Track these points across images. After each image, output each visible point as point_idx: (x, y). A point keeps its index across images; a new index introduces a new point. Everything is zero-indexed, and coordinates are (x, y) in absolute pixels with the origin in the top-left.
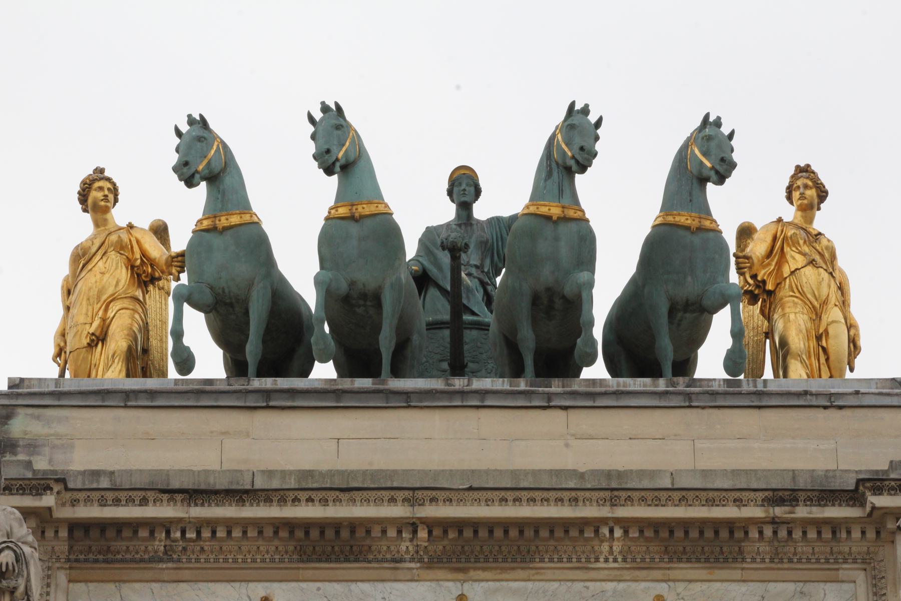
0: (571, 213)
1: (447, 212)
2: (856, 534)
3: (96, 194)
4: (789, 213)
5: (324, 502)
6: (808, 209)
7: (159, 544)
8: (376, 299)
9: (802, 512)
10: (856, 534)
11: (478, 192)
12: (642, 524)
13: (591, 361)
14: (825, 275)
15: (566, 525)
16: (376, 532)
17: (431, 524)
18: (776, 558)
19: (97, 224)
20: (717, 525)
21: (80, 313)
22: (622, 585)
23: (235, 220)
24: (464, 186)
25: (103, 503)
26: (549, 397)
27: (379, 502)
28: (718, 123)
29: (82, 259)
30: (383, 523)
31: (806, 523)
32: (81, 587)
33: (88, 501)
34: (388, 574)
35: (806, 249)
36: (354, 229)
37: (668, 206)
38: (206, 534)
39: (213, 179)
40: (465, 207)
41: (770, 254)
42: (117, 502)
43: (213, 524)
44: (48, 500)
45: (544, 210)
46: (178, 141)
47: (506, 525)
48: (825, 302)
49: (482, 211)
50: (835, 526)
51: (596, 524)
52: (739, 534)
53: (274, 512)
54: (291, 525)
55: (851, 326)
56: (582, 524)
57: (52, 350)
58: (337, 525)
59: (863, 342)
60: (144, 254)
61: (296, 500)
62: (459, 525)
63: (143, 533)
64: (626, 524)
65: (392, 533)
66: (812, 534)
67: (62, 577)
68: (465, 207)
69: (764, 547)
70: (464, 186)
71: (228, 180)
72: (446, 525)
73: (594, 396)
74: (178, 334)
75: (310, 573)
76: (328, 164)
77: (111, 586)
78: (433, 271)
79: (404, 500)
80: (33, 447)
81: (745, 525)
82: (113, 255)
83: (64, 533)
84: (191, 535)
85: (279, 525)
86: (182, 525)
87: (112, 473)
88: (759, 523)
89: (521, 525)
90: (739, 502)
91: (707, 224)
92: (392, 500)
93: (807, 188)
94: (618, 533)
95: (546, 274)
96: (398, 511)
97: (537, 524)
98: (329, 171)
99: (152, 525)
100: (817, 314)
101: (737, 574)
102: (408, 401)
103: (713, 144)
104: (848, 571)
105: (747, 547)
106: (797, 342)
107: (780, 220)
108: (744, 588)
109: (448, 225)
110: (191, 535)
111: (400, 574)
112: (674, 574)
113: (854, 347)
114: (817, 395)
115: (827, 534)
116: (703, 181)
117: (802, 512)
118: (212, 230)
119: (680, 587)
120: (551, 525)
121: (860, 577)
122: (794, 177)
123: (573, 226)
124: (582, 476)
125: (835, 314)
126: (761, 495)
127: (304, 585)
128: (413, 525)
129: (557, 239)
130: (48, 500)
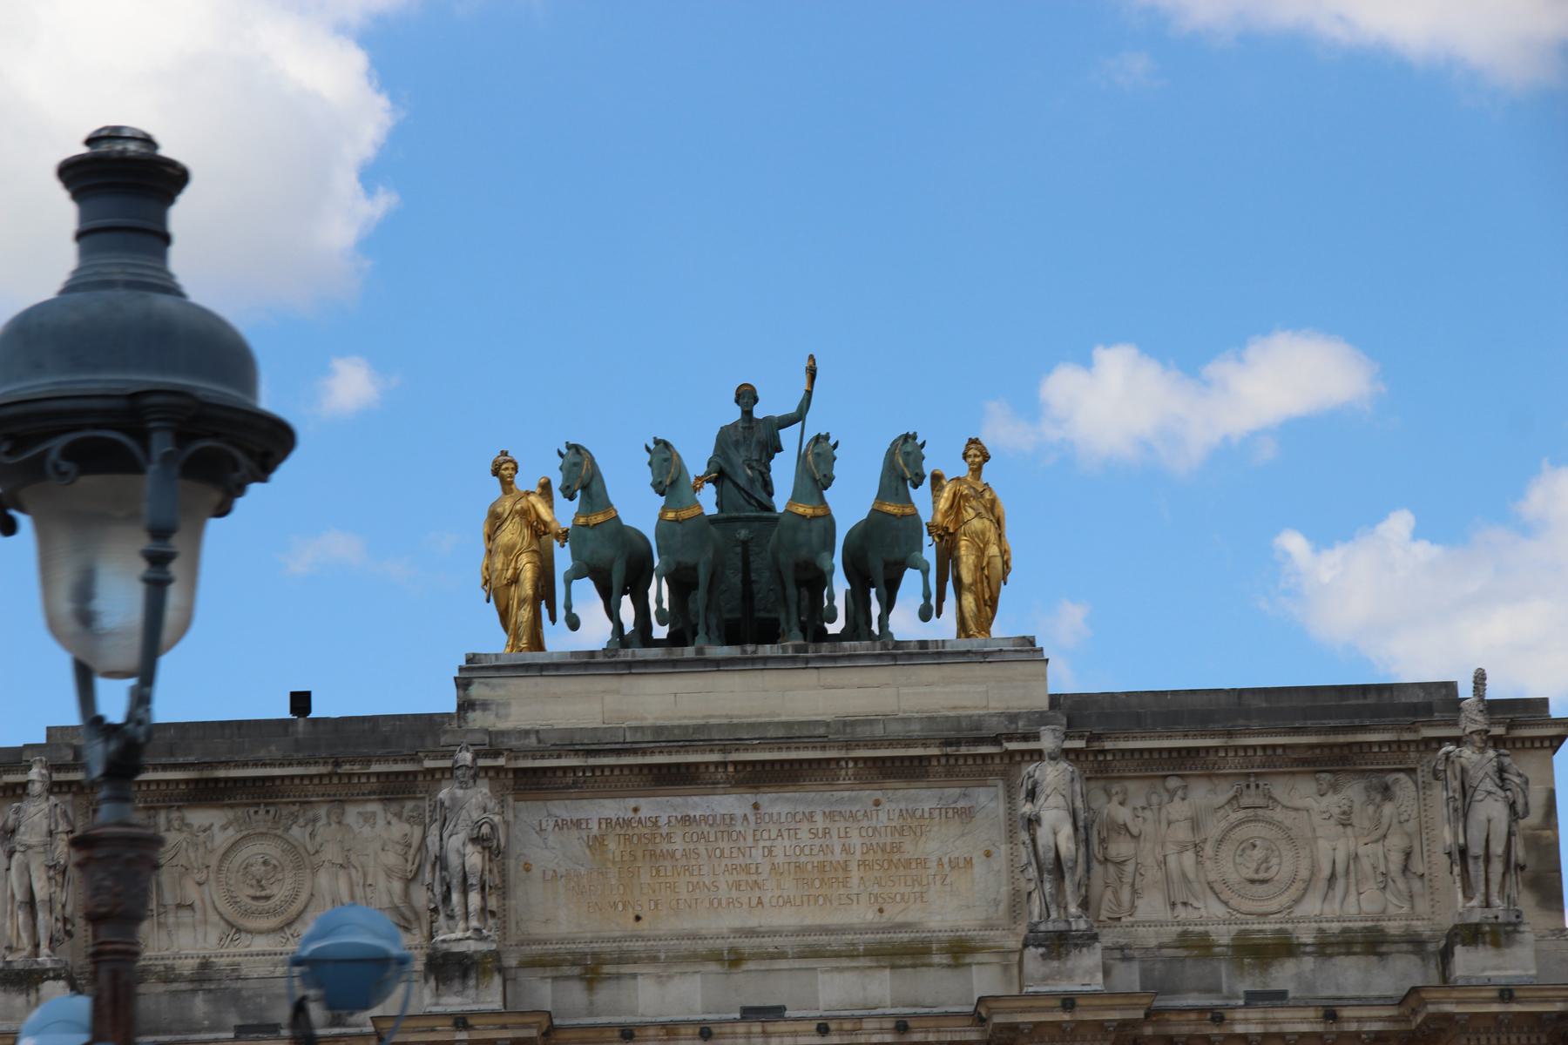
0: (819, 512)
1: (734, 414)
2: (997, 760)
3: (504, 470)
4: (963, 470)
5: (670, 753)
6: (977, 471)
7: (569, 779)
8: (695, 568)
9: (964, 750)
10: (997, 760)
11: (756, 400)
12: (865, 760)
13: (832, 620)
14: (987, 523)
15: (819, 761)
16: (702, 769)
17: (735, 763)
19: (505, 492)
20: (911, 758)
21: (499, 562)
23: (600, 518)
24: (746, 396)
25: (534, 758)
26: (807, 660)
27: (703, 752)
28: (914, 437)
29: (496, 521)
30: (707, 764)
31: (966, 756)
32: (521, 804)
33: (525, 757)
35: (974, 503)
36: (678, 528)
37: (881, 497)
39: (585, 488)
40: (747, 413)
41: (951, 506)
42: (543, 757)
43: (602, 768)
44: (501, 761)
45: (801, 510)
46: (560, 461)
48: (986, 543)
49: (759, 412)
50: (984, 756)
53: (640, 760)
54: (650, 767)
55: (1004, 552)
56: (828, 760)
57: (480, 581)
58: (678, 765)
59: (1012, 564)
60: (538, 516)
61: (652, 753)
62: (753, 763)
63: (560, 774)
64: (856, 760)
65: (712, 769)
66: (970, 761)
67: (510, 799)
68: (747, 413)
70: (746, 396)
71: (595, 487)
72: (745, 763)
74: (568, 607)
76: (660, 488)
77: (540, 803)
78: (728, 469)
80: (485, 705)
81: (929, 758)
82: (517, 519)
83: (511, 775)
85: (641, 767)
86: (584, 769)
87: (537, 732)
88: (938, 757)
90: (925, 745)
91: (908, 511)
92: (712, 751)
93: (977, 454)
95: (804, 554)
96: (715, 757)
97: (801, 762)
98: (662, 494)
99: (565, 769)
100: (981, 552)
101: (924, 784)
102: (718, 664)
103: (911, 458)
104: (991, 780)
106: (967, 578)
107: (958, 479)
108: (929, 792)
109: (735, 425)
112: (887, 785)
113: (1006, 564)
114: (976, 653)
115: (979, 761)
116: (904, 480)
117: (964, 750)
118: (586, 525)
119: (890, 793)
120: (810, 761)
121: (1000, 784)
122: (968, 448)
123: (821, 521)
124: (827, 724)
125: (993, 550)
128: (725, 764)
129: (810, 531)
130: (501, 761)
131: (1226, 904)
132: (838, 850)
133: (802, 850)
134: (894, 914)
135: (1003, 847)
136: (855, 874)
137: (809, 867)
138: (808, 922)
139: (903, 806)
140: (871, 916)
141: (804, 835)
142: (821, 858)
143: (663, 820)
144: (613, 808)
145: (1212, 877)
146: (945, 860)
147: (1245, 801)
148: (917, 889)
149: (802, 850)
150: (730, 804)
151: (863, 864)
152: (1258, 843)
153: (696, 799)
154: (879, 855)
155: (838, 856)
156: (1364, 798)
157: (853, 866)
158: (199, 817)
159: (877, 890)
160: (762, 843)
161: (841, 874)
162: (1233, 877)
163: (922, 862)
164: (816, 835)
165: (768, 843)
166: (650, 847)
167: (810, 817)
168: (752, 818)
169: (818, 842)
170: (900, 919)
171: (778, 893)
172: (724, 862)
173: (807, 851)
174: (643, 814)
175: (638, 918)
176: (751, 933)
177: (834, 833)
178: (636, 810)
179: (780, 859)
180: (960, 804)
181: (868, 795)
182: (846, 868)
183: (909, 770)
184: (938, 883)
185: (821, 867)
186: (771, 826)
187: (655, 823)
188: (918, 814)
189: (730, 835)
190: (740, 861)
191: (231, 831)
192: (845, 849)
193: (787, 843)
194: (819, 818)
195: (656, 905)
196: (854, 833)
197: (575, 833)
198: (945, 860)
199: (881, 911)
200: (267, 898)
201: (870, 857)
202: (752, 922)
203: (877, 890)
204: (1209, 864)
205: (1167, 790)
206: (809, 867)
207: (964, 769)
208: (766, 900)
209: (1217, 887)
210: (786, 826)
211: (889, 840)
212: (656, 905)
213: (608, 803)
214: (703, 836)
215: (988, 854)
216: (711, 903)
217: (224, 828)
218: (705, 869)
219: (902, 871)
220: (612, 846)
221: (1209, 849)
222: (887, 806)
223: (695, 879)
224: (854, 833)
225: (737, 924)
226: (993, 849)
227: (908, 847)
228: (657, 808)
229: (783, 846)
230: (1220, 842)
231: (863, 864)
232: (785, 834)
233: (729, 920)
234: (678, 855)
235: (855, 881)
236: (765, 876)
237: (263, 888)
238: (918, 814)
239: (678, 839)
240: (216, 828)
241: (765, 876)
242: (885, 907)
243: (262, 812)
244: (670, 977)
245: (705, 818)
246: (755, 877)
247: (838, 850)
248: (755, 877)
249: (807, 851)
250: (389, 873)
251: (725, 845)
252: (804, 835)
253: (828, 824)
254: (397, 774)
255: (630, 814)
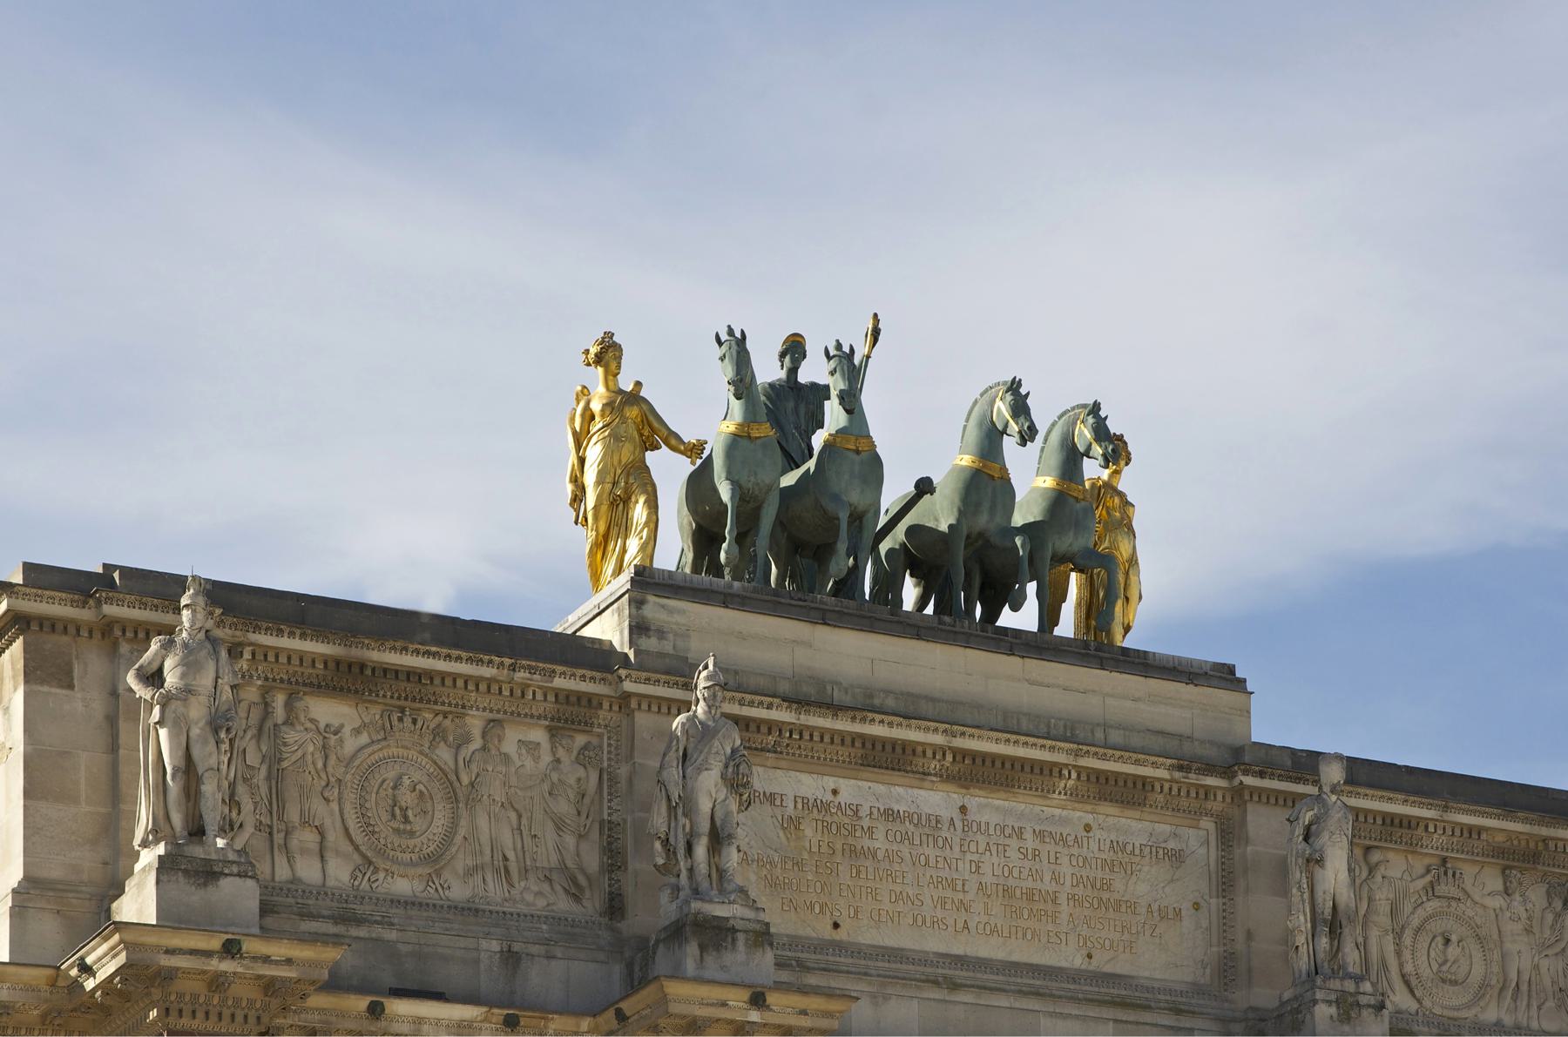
10: (1220, 798)
18: (1165, 807)
22: (1065, 813)
34: (917, 783)
38: (807, 737)
47: (1004, 759)
50: (1208, 792)
51: (1060, 767)
52: (1148, 788)
53: (858, 728)
54: (863, 738)
58: (894, 743)
62: (974, 756)
69: (1161, 798)
73: (1015, 642)
75: (865, 775)
79: (945, 731)
84: (796, 736)
85: (855, 737)
89: (1014, 760)
94: (1074, 775)
96: (939, 739)
101: (1137, 814)
105: (1152, 797)
110: (796, 736)
111: (926, 784)
126: (1169, 761)
127: (860, 783)
131: (1419, 1001)
132: (1047, 878)
133: (1011, 872)
134: (1102, 962)
135: (1213, 901)
136: (1065, 908)
137: (1018, 893)
138: (1015, 958)
139: (1113, 837)
140: (1078, 962)
141: (1013, 854)
142: (1030, 884)
143: (864, 812)
144: (811, 785)
145: (1409, 968)
146: (1155, 907)
147: (1442, 889)
148: (1126, 936)
149: (1011, 872)
150: (936, 800)
151: (1072, 898)
152: (1454, 938)
153: (900, 790)
154: (1089, 891)
155: (1048, 885)
156: (1545, 904)
157: (1062, 899)
158: (325, 710)
159: (1085, 931)
160: (969, 857)
161: (1050, 907)
162: (1426, 972)
163: (1132, 907)
164: (1026, 856)
165: (975, 857)
166: (850, 840)
167: (1019, 833)
168: (958, 824)
169: (1027, 864)
170: (1108, 969)
171: (984, 919)
172: (929, 872)
173: (1016, 874)
174: (843, 797)
175: (836, 926)
176: (960, 961)
177: (1044, 856)
178: (835, 792)
179: (988, 879)
180: (1171, 845)
181: (1079, 815)
182: (1054, 901)
183: (1128, 793)
184: (1148, 933)
185: (1030, 896)
186: (980, 838)
187: (856, 812)
188: (1129, 848)
189: (935, 841)
190: (945, 873)
191: (364, 739)
192: (1056, 878)
193: (995, 860)
194: (1028, 835)
195: (856, 912)
196: (1065, 860)
197: (767, 807)
198: (1155, 907)
199: (1090, 956)
200: (412, 834)
201: (1080, 891)
202: (958, 950)
203: (1085, 931)
204: (1407, 955)
205: (1367, 863)
206: (1018, 893)
207: (1184, 803)
208: (972, 925)
209: (1414, 982)
210: (994, 839)
211: (1100, 874)
212: (856, 912)
213: (805, 778)
214: (906, 838)
215: (1197, 907)
216: (915, 920)
217: (357, 732)
218: (909, 878)
219: (1111, 914)
220: (809, 832)
221: (1407, 940)
222: (1097, 833)
223: (898, 889)
224: (1065, 860)
225: (942, 949)
226: (1203, 903)
227: (1118, 885)
228: (860, 791)
229: (991, 862)
230: (1418, 930)
231: (1072, 898)
232: (994, 849)
233: (934, 943)
234: (880, 855)
235: (1064, 917)
236: (971, 896)
237: (406, 820)
238: (1129, 848)
239: (880, 834)
240: (347, 730)
241: (971, 896)
242: (1094, 952)
243: (408, 720)
244: (887, 998)
245: (910, 816)
246: (961, 896)
247: (1047, 878)
248: (961, 896)
249: (1016, 874)
250: (559, 826)
251: (931, 852)
252: (1013, 854)
253: (1037, 844)
254: (580, 696)
255: (829, 797)
